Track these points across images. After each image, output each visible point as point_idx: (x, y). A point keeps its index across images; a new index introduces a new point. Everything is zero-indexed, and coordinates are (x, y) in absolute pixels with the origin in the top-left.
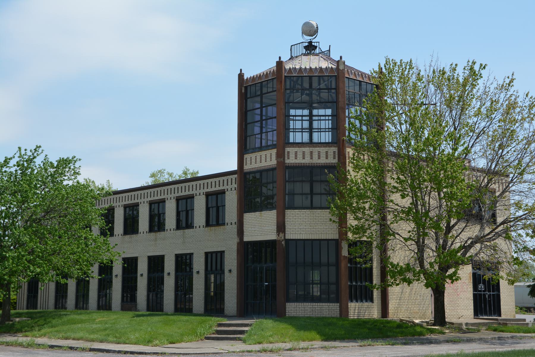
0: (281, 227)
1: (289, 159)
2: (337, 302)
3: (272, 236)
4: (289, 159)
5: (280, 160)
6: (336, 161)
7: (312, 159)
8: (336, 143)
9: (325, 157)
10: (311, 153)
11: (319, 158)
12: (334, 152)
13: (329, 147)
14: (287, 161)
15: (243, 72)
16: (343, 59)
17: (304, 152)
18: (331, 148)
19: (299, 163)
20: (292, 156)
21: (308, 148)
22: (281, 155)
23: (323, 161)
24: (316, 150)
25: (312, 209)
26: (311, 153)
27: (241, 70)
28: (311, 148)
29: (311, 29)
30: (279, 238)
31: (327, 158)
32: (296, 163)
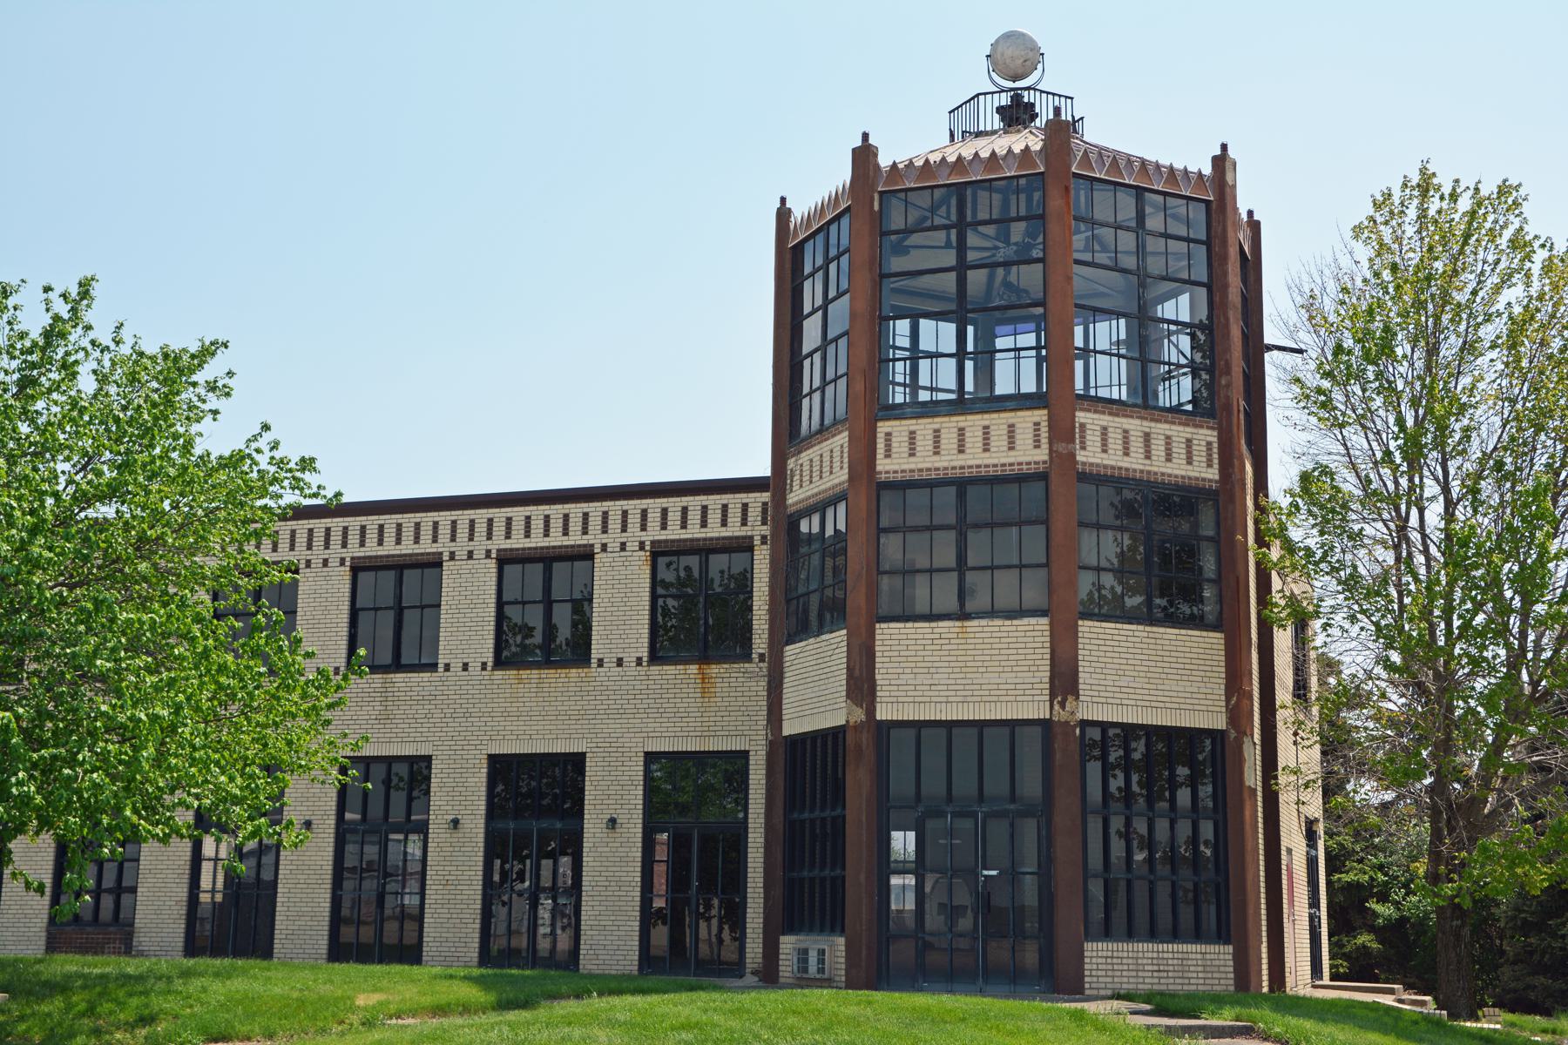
0: (1064, 681)
1: (1083, 448)
2: (1227, 942)
3: (1035, 707)
4: (1083, 448)
5: (1061, 447)
6: (1213, 474)
7: (1148, 457)
8: (1210, 414)
9: (1181, 455)
10: (1147, 437)
11: (1169, 458)
12: (1209, 444)
13: (1196, 426)
14: (1081, 457)
15: (872, 141)
16: (1231, 153)
17: (1126, 431)
18: (1202, 431)
19: (1113, 468)
20: (1093, 439)
21: (1138, 422)
22: (1063, 433)
23: (1178, 469)
24: (1160, 429)
25: (1151, 625)
26: (1147, 437)
27: (865, 136)
28: (1146, 423)
29: (1031, 54)
30: (1060, 715)
31: (1189, 461)
32: (1105, 467)
